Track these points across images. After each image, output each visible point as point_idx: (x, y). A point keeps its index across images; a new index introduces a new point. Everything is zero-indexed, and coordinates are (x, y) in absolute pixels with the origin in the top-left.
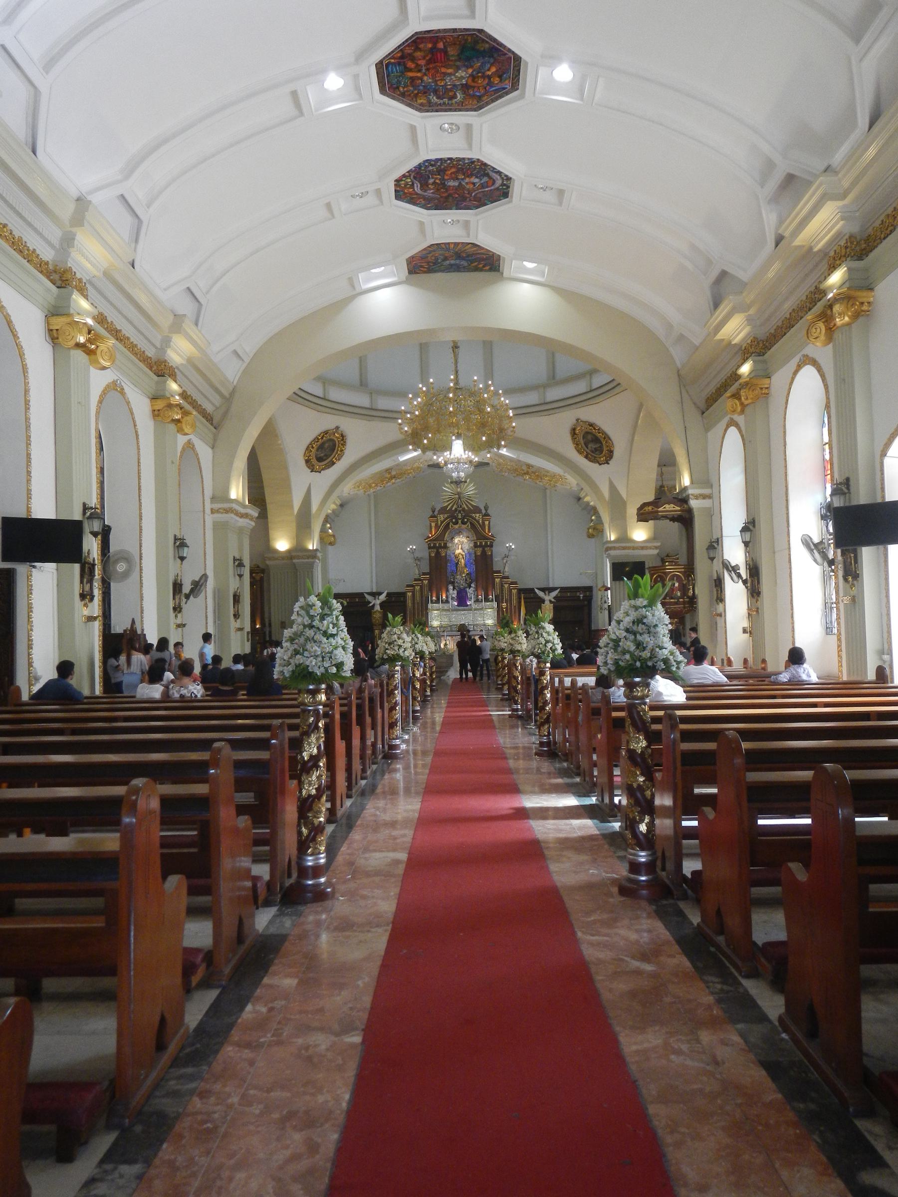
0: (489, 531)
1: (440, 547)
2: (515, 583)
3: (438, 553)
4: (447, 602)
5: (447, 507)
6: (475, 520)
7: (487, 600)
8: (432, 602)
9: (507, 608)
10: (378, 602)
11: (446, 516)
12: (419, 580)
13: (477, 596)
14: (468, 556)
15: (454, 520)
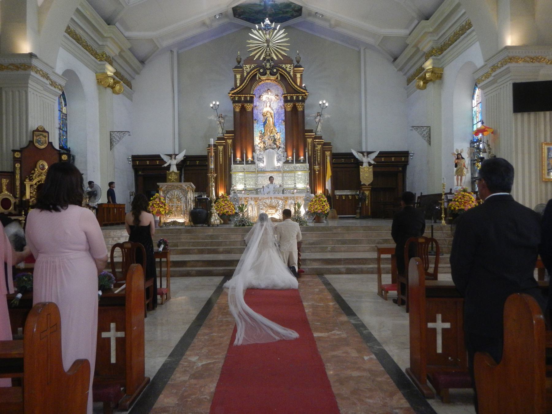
0: (301, 82)
1: (246, 101)
2: (329, 144)
3: (243, 109)
4: (253, 162)
5: (254, 56)
6: (286, 71)
7: (298, 161)
8: (235, 162)
9: (319, 171)
10: (174, 162)
11: (253, 66)
12: (222, 139)
13: (287, 157)
14: (276, 116)
15: (261, 71)
